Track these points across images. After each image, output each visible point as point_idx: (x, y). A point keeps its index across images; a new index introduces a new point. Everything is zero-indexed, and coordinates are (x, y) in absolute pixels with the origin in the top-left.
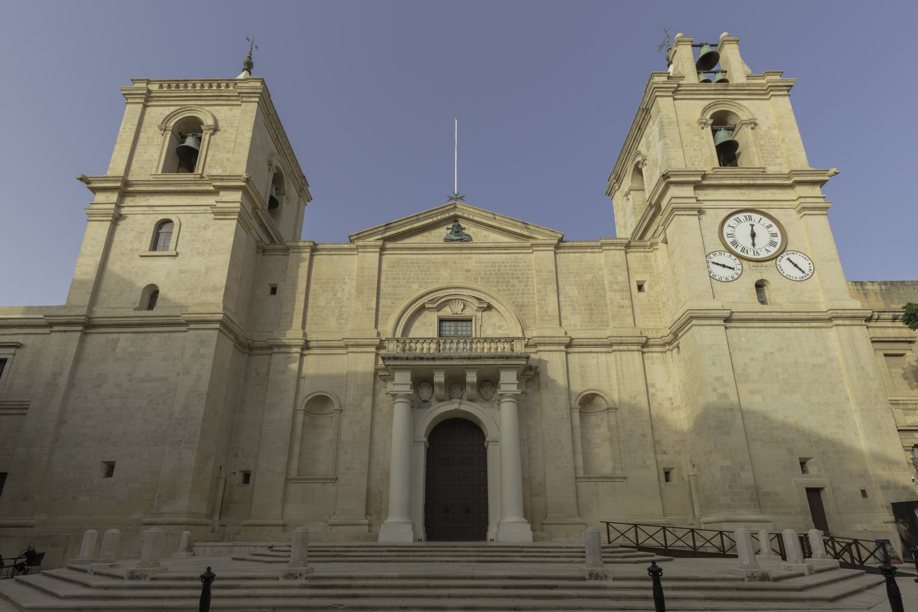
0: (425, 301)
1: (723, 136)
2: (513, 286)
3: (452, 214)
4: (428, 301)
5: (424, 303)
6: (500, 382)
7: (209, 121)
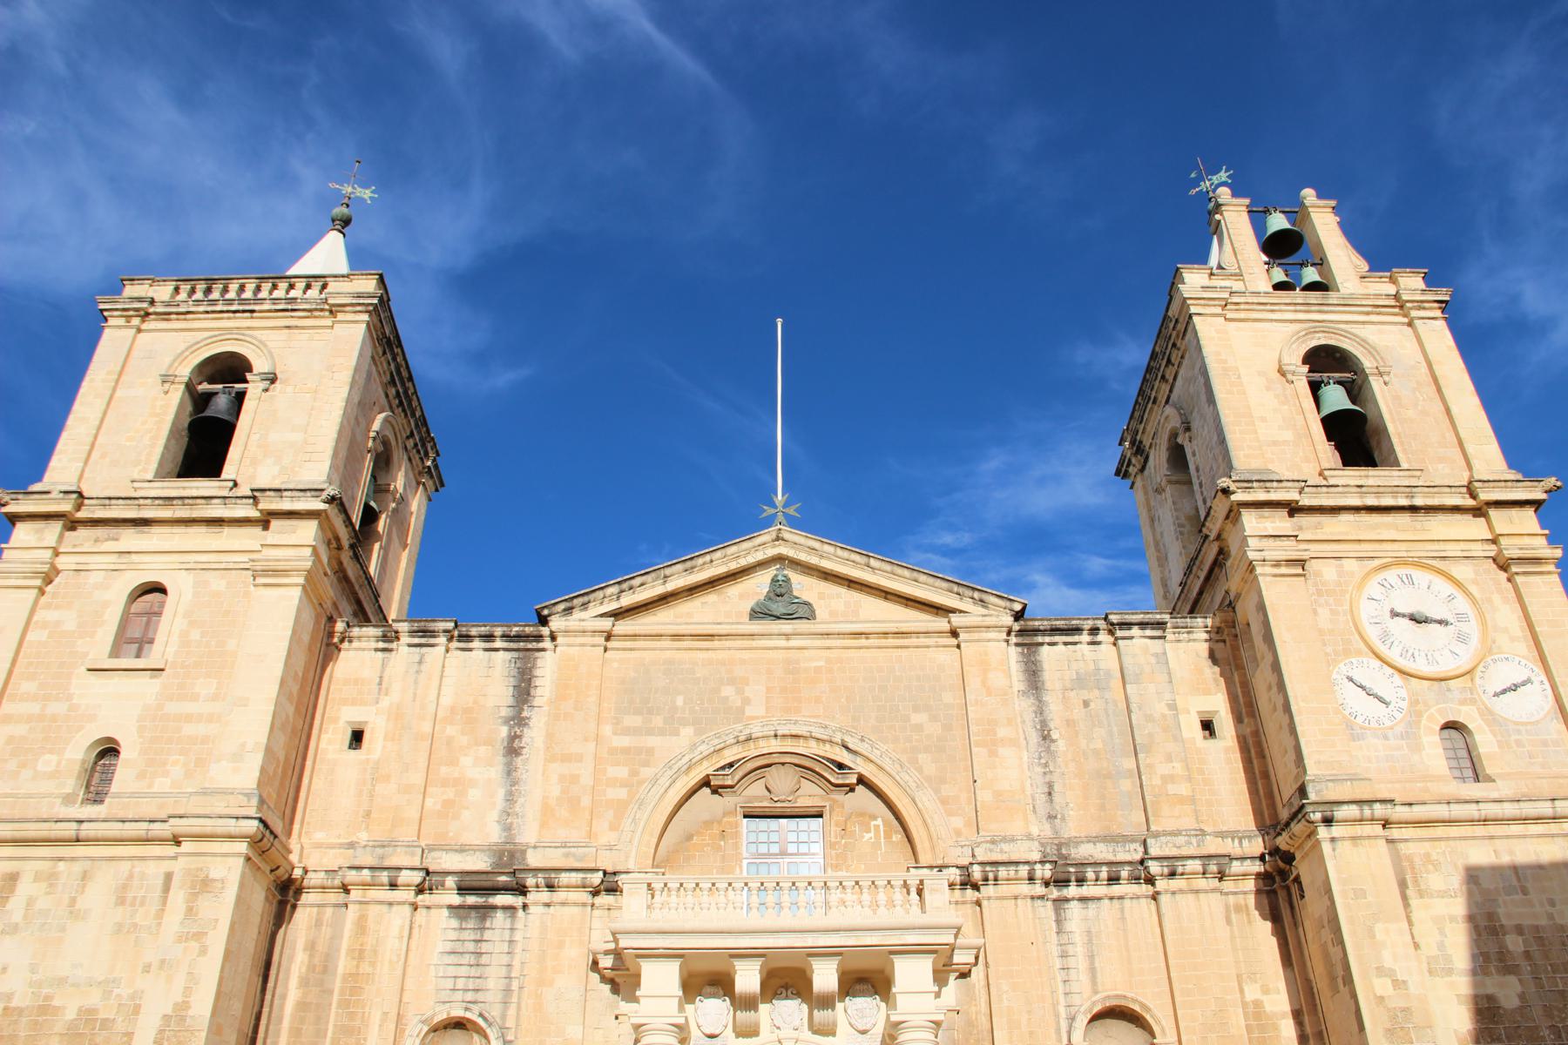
0: (710, 771)
1: (1336, 399)
2: (918, 728)
3: (771, 552)
4: (717, 770)
5: (708, 776)
6: (894, 990)
7: (260, 364)
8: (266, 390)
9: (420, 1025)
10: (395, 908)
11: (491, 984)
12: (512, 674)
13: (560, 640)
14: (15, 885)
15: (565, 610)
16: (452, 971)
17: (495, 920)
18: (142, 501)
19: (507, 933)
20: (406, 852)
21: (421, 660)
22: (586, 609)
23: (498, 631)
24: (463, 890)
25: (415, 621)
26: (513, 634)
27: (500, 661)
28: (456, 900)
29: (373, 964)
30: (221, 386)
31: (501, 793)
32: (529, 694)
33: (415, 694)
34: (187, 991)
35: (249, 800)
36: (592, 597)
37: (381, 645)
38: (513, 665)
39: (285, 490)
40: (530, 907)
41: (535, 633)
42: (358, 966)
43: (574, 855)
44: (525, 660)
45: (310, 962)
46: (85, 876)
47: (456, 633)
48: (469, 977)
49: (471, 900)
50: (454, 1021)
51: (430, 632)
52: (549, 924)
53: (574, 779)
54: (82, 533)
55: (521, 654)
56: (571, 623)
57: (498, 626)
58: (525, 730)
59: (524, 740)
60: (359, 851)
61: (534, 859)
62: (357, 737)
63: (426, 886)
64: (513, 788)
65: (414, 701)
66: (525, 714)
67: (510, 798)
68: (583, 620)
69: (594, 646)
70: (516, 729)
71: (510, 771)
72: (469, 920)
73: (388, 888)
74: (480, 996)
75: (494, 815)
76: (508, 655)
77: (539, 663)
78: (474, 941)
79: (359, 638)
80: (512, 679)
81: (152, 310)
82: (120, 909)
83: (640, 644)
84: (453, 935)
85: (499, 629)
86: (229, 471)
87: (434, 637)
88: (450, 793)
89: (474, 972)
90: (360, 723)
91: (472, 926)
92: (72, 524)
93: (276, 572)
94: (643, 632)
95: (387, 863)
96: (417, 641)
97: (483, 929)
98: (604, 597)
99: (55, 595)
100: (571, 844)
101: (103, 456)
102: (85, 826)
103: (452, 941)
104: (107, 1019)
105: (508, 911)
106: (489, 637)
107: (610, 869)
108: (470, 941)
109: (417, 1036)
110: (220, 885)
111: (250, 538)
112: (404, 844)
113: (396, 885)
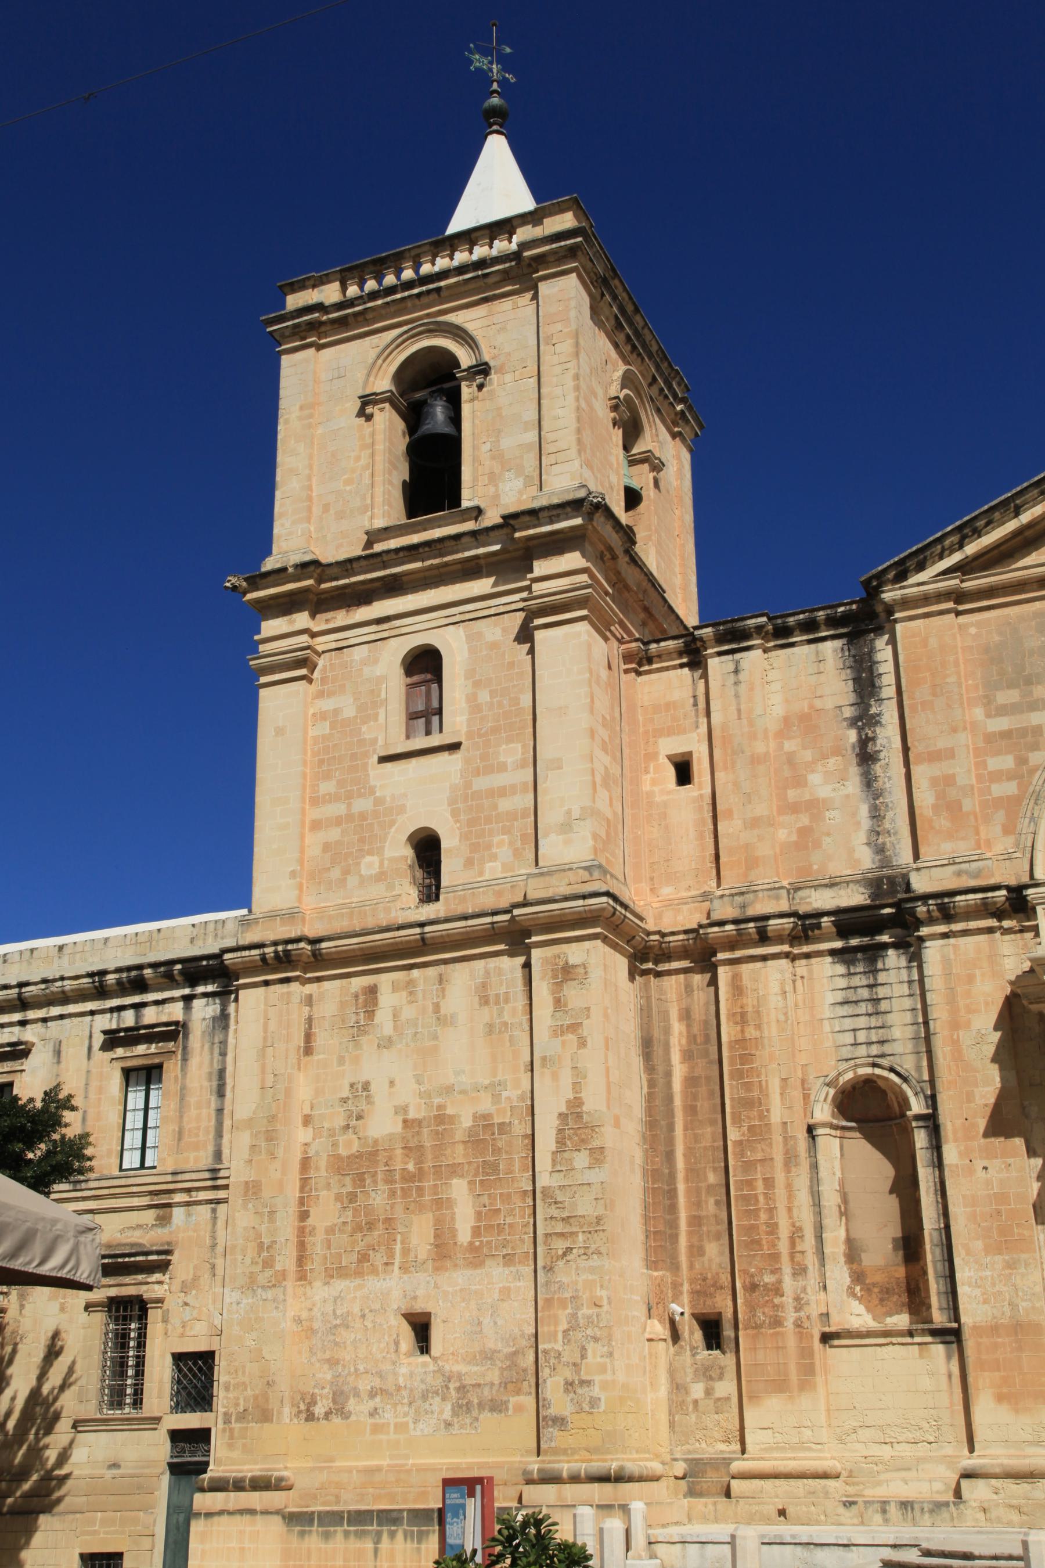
9: (826, 1088)
11: (897, 1033)
14: (376, 998)
16: (849, 1023)
17: (887, 961)
21: (736, 668)
24: (843, 931)
28: (838, 944)
29: (758, 1027)
31: (864, 810)
33: (739, 711)
43: (966, 872)
45: (688, 1032)
46: (441, 979)
48: (870, 1028)
49: (854, 942)
50: (863, 1078)
52: (952, 957)
53: (949, 780)
58: (878, 730)
59: (879, 742)
60: (717, 903)
61: (920, 884)
62: (684, 772)
65: (739, 718)
67: (876, 815)
71: (869, 782)
74: (887, 1048)
75: (861, 837)
84: (842, 983)
88: (804, 820)
89: (874, 1021)
90: (683, 754)
91: (862, 970)
95: (751, 912)
97: (875, 972)
102: (427, 929)
107: (1013, 882)
108: (863, 987)
109: (825, 1100)
112: (765, 887)
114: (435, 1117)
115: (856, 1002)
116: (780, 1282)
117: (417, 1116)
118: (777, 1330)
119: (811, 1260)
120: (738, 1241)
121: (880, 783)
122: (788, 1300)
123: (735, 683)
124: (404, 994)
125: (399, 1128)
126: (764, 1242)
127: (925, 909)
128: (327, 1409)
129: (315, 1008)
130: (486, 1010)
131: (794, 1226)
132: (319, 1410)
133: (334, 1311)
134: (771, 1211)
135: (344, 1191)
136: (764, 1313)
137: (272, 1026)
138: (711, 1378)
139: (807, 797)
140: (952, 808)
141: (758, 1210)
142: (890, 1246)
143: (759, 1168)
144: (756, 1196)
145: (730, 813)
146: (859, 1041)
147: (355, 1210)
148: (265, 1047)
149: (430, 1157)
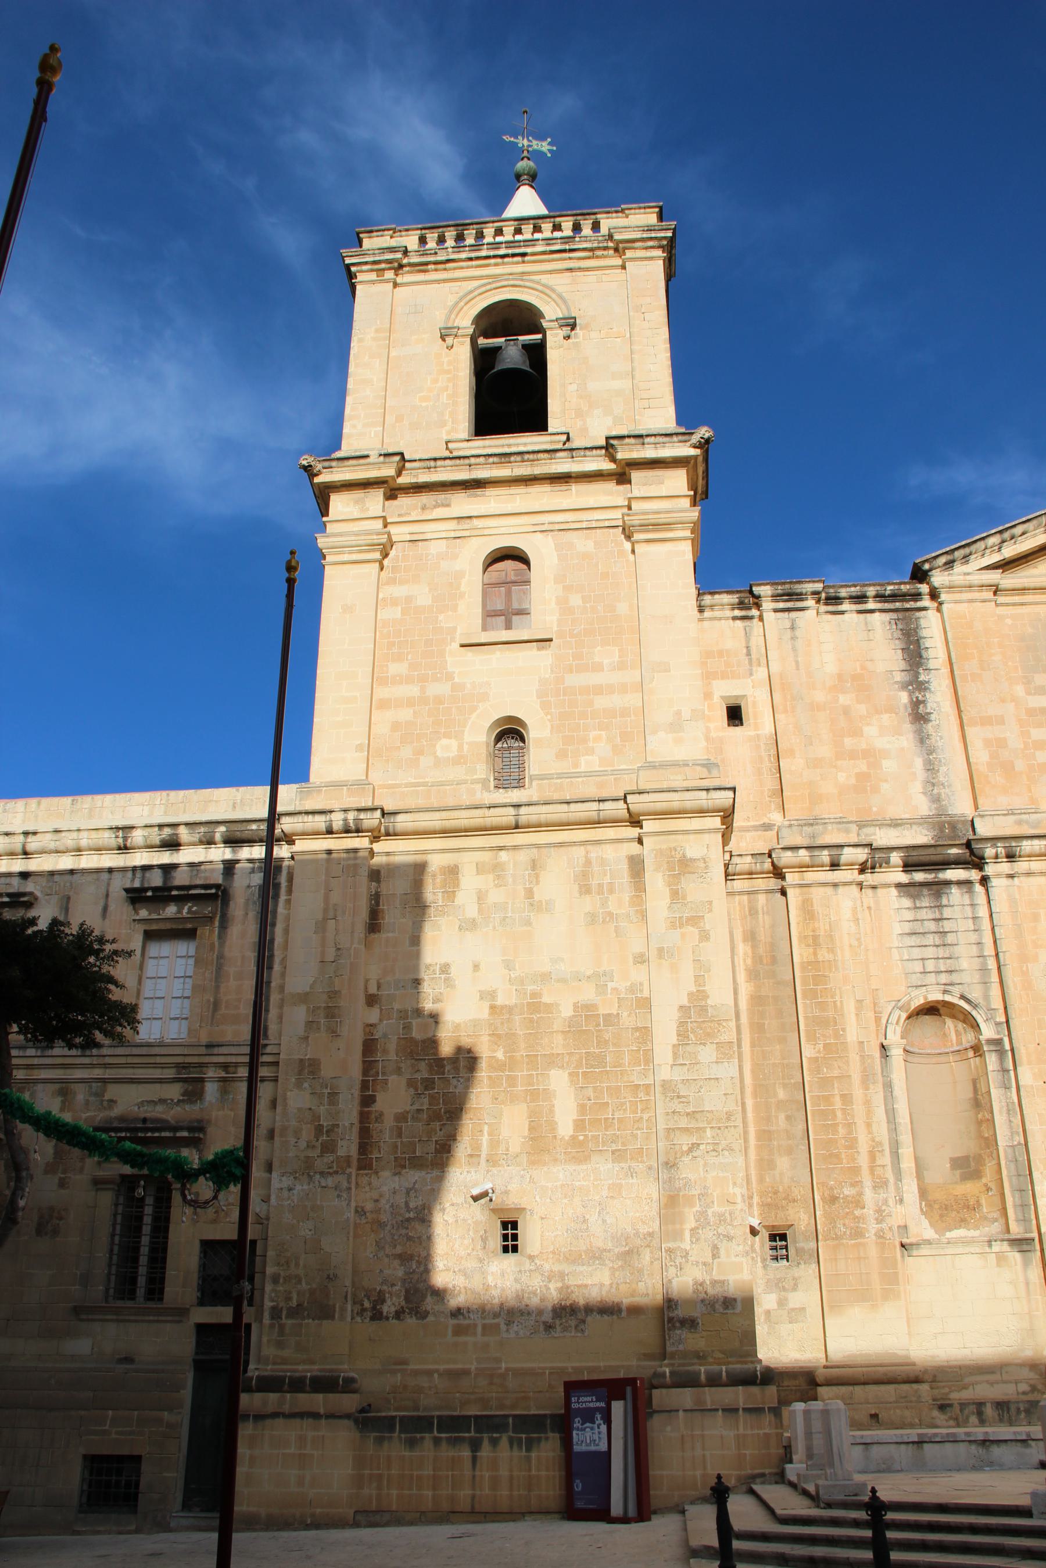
8: (567, 337)
10: (841, 889)
11: (964, 964)
12: (895, 635)
13: (943, 597)
15: (946, 564)
18: (473, 460)
19: (968, 909)
20: (839, 830)
21: (793, 625)
22: (967, 562)
23: (871, 591)
24: (908, 866)
25: (777, 584)
26: (888, 593)
27: (878, 623)
28: (904, 878)
29: (831, 950)
30: (503, 340)
31: (919, 763)
32: (921, 657)
33: (797, 662)
34: (699, 979)
35: (709, 771)
36: (973, 548)
37: (737, 613)
38: (894, 627)
39: (647, 436)
40: (992, 880)
41: (913, 591)
42: (815, 954)
43: (1027, 822)
44: (907, 621)
46: (534, 865)
47: (823, 595)
48: (938, 958)
49: (920, 876)
51: (797, 594)
52: (1017, 897)
53: (1002, 743)
54: (404, 502)
55: (901, 615)
56: (954, 578)
57: (870, 585)
59: (928, 705)
61: (984, 829)
63: (869, 864)
64: (931, 757)
65: (798, 668)
66: (922, 678)
67: (931, 768)
68: (968, 574)
69: (984, 601)
70: (917, 694)
71: (922, 739)
72: (922, 898)
73: (828, 868)
74: (955, 978)
75: (917, 787)
76: (887, 617)
77: (923, 623)
78: (933, 920)
79: (712, 607)
80: (897, 642)
81: (405, 261)
82: (588, 898)
83: (1029, 598)
84: (909, 915)
85: (871, 588)
86: (554, 423)
87: (802, 600)
89: (941, 952)
90: (737, 697)
91: (928, 905)
92: (393, 492)
93: (657, 526)
94: (1032, 585)
95: (820, 842)
96: (781, 605)
97: (940, 907)
98: (986, 548)
99: (395, 569)
100: (1019, 811)
101: (399, 419)
103: (909, 921)
104: (610, 1015)
105: (963, 886)
106: (861, 598)
109: (897, 1023)
110: (702, 865)
111: (609, 493)
113: (838, 865)
114: (529, 1004)
115: (924, 934)
116: (861, 1194)
117: (507, 1003)
118: (859, 1240)
119: (890, 1176)
120: (816, 1154)
121: (933, 740)
122: (869, 1211)
123: (792, 638)
124: (491, 877)
125: (485, 1014)
126: (843, 1156)
127: (994, 851)
128: (398, 1308)
129: (383, 885)
130: (588, 898)
131: (874, 1141)
132: (388, 1308)
133: (407, 1204)
134: (850, 1126)
135: (418, 1076)
136: (844, 1225)
137: (335, 897)
138: (784, 1289)
139: (864, 746)
140: (1008, 768)
141: (837, 1125)
142: (948, 1165)
143: (836, 1085)
144: (833, 1111)
145: (791, 752)
146: (927, 971)
147: (431, 1097)
148: (325, 919)
149: (523, 1045)
